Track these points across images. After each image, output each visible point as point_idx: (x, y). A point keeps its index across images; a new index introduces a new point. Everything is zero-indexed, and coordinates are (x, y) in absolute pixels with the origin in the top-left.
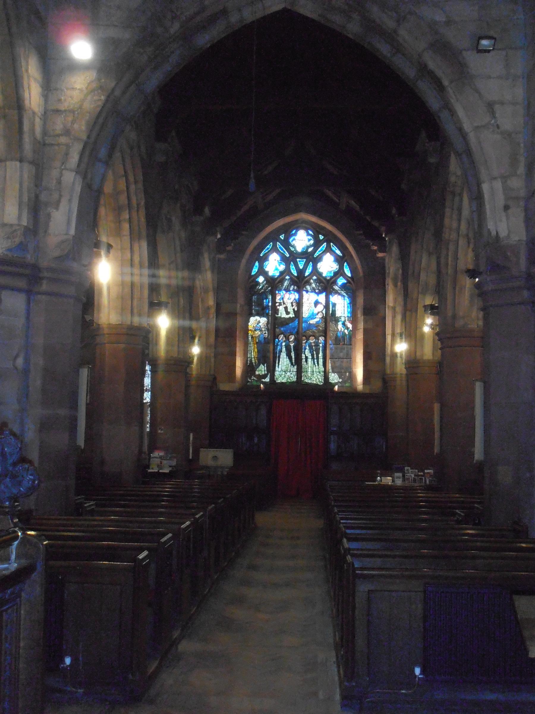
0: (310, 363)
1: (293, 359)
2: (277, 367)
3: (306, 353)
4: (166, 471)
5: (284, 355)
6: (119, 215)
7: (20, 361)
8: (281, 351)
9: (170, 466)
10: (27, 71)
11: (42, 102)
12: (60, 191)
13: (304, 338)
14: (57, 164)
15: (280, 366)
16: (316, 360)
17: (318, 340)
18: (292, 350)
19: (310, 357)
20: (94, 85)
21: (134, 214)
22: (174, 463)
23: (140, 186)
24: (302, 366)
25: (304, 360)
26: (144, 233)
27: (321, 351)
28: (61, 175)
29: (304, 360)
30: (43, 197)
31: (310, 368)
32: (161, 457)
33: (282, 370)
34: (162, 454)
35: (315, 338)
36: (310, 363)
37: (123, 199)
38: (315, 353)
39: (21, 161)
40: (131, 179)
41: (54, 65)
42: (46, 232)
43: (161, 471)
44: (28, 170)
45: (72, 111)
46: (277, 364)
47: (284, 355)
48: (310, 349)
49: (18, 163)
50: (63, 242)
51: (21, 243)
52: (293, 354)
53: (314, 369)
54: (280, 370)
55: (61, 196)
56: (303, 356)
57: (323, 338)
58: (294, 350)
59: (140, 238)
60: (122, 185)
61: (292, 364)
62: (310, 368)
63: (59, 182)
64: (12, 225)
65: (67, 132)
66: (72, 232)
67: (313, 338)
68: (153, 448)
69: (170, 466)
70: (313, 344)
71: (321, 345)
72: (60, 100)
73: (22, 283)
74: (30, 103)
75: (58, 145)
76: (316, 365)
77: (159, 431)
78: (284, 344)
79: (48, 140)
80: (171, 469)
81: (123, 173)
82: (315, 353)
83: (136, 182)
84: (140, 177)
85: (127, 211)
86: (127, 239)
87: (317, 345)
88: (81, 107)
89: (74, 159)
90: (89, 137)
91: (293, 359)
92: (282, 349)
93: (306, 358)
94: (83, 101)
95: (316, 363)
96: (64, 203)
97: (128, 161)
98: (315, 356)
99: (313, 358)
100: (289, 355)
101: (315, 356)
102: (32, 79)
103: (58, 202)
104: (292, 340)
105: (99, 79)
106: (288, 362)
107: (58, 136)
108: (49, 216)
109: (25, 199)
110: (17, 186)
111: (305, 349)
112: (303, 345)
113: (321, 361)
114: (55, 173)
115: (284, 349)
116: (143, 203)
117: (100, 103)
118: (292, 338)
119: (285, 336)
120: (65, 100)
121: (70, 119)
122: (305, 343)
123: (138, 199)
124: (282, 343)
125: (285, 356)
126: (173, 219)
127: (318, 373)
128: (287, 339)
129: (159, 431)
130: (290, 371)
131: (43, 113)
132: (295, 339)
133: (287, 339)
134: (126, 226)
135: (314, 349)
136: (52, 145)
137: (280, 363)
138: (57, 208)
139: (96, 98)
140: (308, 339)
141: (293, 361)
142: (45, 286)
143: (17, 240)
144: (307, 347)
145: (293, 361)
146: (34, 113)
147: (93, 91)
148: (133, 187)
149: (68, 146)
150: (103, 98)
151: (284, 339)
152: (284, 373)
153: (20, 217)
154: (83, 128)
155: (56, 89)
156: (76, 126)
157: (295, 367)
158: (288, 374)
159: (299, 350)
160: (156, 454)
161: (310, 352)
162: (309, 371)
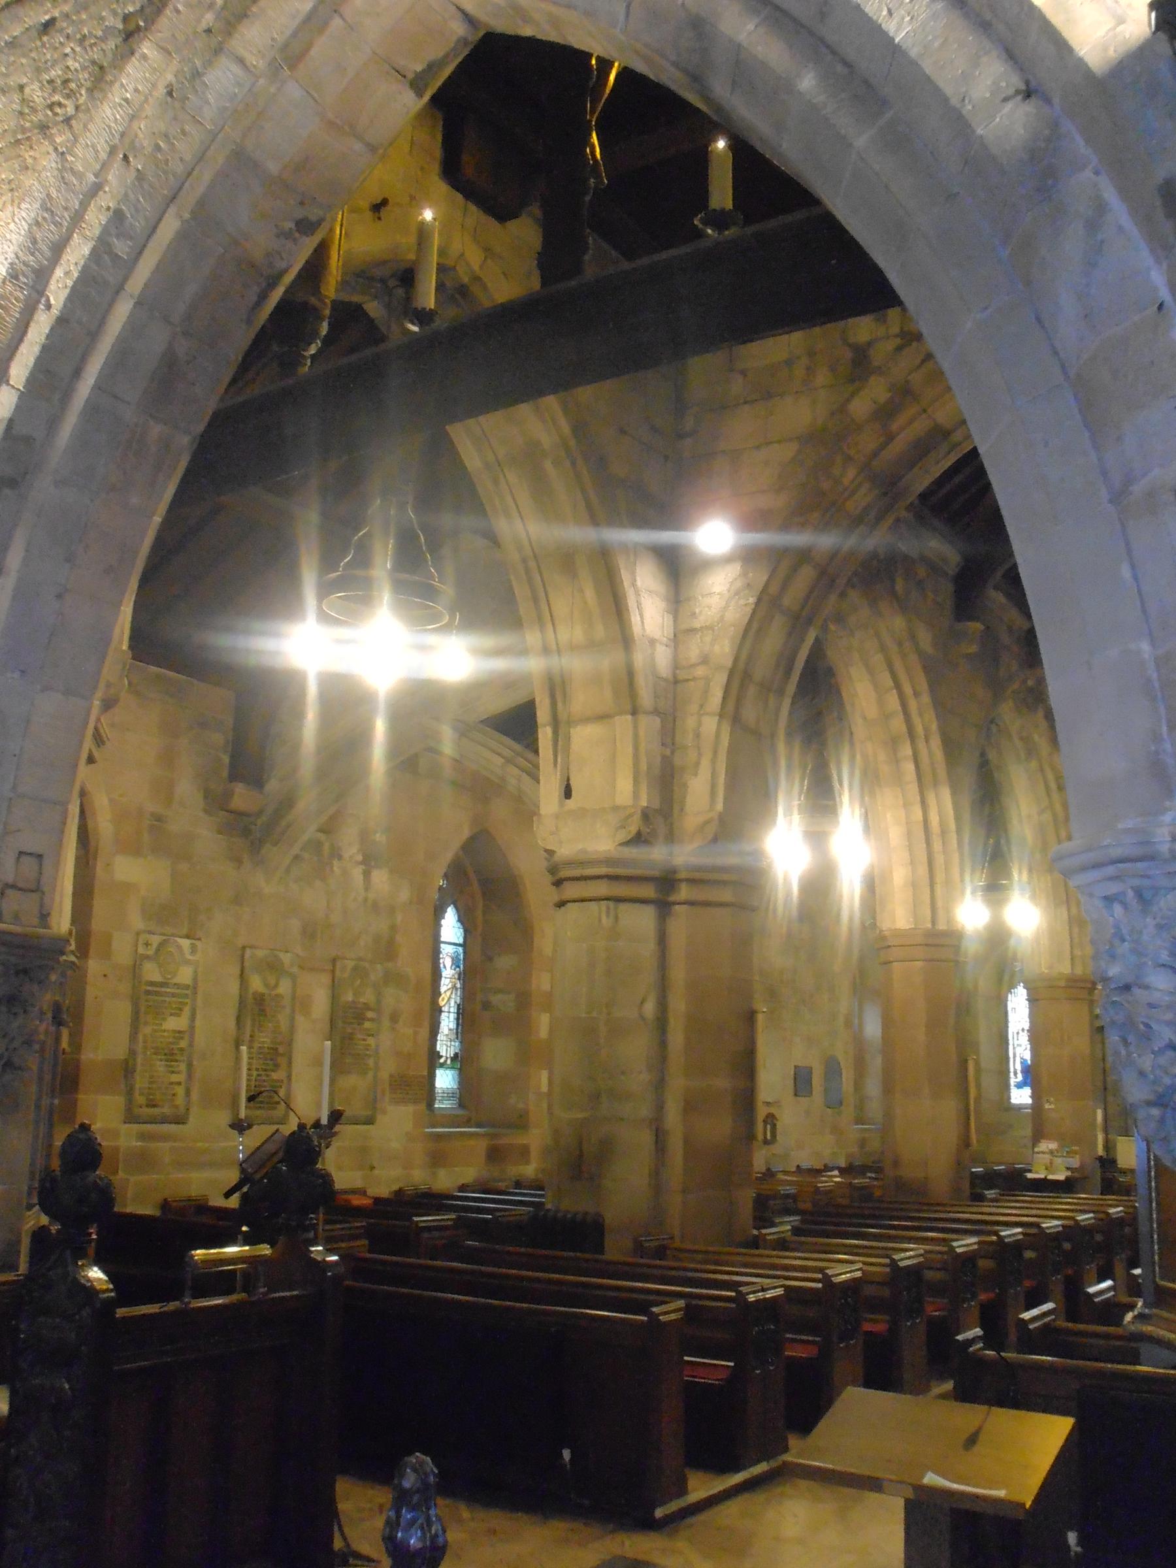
4: (1061, 1176)
6: (895, 751)
7: (650, 1008)
9: (1068, 1169)
10: (634, 584)
11: (668, 620)
12: (699, 748)
14: (694, 708)
20: (739, 584)
21: (921, 745)
22: (1075, 1162)
23: (926, 699)
26: (942, 772)
28: (700, 724)
30: (677, 761)
32: (1051, 1152)
34: (1053, 1146)
37: (898, 724)
39: (634, 712)
40: (908, 689)
41: (677, 567)
42: (682, 810)
43: (1050, 1177)
44: (649, 725)
45: (710, 628)
49: (629, 717)
50: (707, 822)
51: (639, 834)
55: (700, 755)
59: (936, 783)
60: (893, 702)
63: (698, 735)
64: (625, 808)
65: (705, 660)
66: (720, 806)
68: (1038, 1135)
69: (1068, 1169)
72: (694, 614)
73: (649, 891)
74: (644, 629)
75: (694, 679)
77: (1047, 1106)
79: (682, 675)
80: (1069, 1173)
81: (891, 683)
83: (916, 694)
84: (924, 686)
85: (908, 742)
86: (913, 788)
88: (722, 618)
89: (717, 695)
90: (736, 660)
94: (726, 608)
96: (705, 763)
97: (898, 665)
102: (642, 594)
103: (697, 764)
105: (744, 574)
107: (694, 666)
108: (685, 785)
109: (644, 767)
110: (630, 750)
114: (691, 722)
116: (934, 726)
117: (749, 610)
120: (701, 612)
121: (708, 639)
123: (926, 720)
126: (1036, 737)
129: (1047, 1106)
131: (672, 636)
134: (909, 767)
136: (687, 680)
138: (696, 775)
139: (742, 602)
142: (684, 892)
143: (633, 829)
146: (652, 642)
147: (737, 593)
148: (913, 705)
149: (707, 680)
150: (752, 600)
153: (636, 795)
154: (727, 650)
155: (688, 599)
156: (717, 648)
160: (1046, 1146)
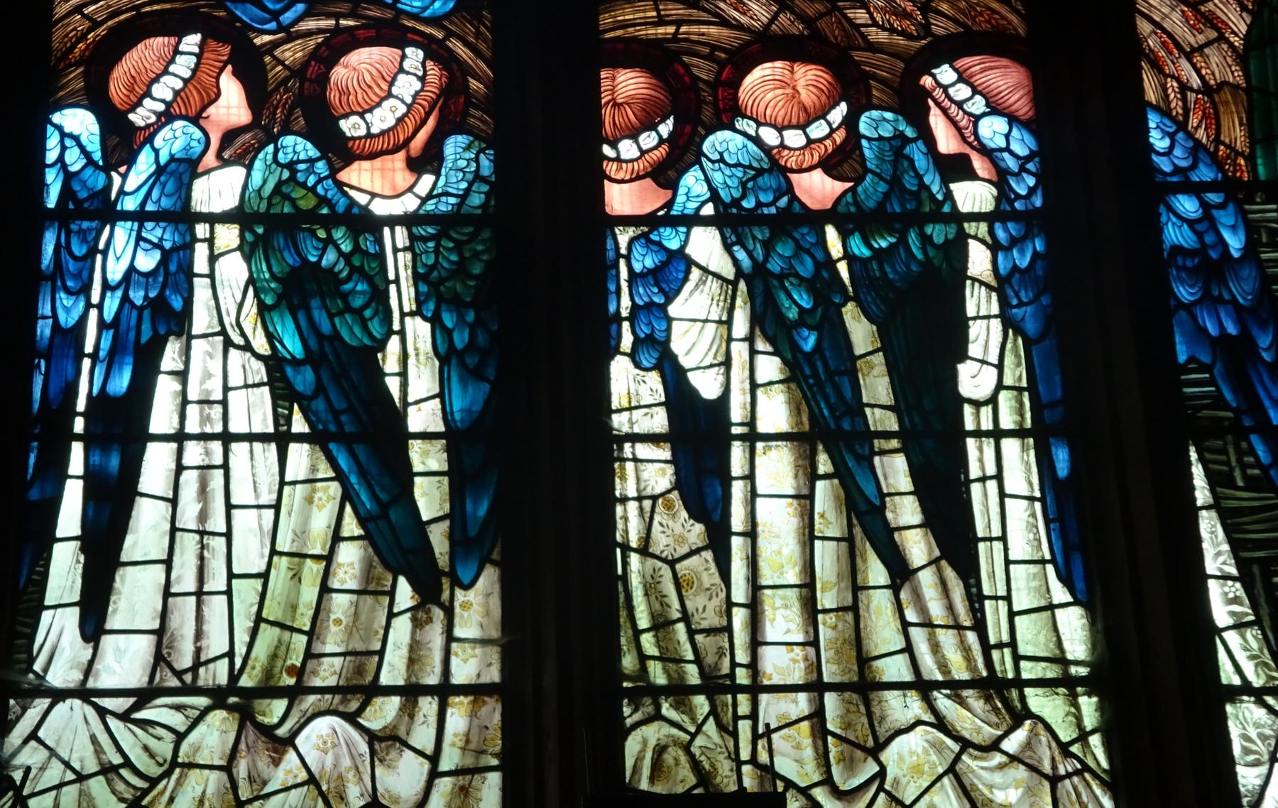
0: (778, 523)
1: (427, 458)
2: (59, 630)
3: (691, 343)
5: (218, 374)
8: (159, 315)
13: (628, 84)
15: (135, 596)
16: (896, 472)
17: (913, 105)
18: (403, 295)
19: (775, 413)
24: (607, 591)
25: (648, 472)
27: (979, 302)
29: (648, 472)
31: (783, 621)
33: (167, 678)
35: (852, 86)
36: (778, 523)
38: (861, 332)
46: (65, 569)
47: (218, 374)
48: (759, 286)
52: (414, 370)
53: (883, 630)
54: (124, 662)
56: (632, 388)
57: (1006, 79)
58: (435, 293)
61: (395, 542)
62: (783, 621)
67: (809, 79)
70: (818, 188)
71: (973, 196)
76: (917, 547)
78: (218, 189)
82: (861, 332)
87: (899, 205)
91: (427, 458)
92: (176, 271)
93: (700, 436)
95: (906, 511)
98: (876, 386)
99: (830, 431)
100: (337, 402)
101: (876, 386)
104: (383, 118)
106: (319, 511)
111: (672, 272)
112: (621, 198)
113: (1009, 489)
115: (226, 279)
118: (386, 85)
119: (250, 70)
122: (665, 173)
124: (183, 171)
125: (252, 411)
127: (971, 718)
128: (298, 103)
130: (359, 690)
132: (450, 109)
133: (298, 103)
135: (850, 307)
137: (146, 529)
140: (697, 100)
141: (430, 498)
144: (705, 246)
145: (430, 498)
151: (232, 105)
152: (214, 735)
157: (477, 606)
158: (322, 739)
159: (536, 291)
161: (769, 323)
162: (781, 664)
